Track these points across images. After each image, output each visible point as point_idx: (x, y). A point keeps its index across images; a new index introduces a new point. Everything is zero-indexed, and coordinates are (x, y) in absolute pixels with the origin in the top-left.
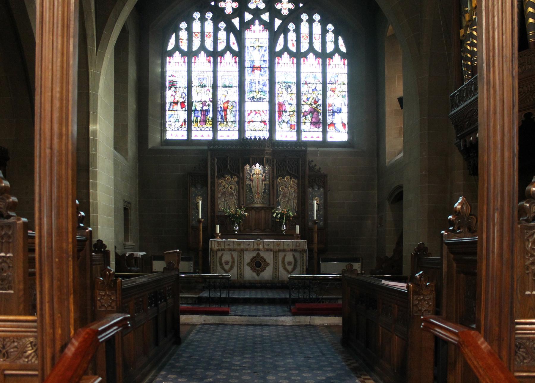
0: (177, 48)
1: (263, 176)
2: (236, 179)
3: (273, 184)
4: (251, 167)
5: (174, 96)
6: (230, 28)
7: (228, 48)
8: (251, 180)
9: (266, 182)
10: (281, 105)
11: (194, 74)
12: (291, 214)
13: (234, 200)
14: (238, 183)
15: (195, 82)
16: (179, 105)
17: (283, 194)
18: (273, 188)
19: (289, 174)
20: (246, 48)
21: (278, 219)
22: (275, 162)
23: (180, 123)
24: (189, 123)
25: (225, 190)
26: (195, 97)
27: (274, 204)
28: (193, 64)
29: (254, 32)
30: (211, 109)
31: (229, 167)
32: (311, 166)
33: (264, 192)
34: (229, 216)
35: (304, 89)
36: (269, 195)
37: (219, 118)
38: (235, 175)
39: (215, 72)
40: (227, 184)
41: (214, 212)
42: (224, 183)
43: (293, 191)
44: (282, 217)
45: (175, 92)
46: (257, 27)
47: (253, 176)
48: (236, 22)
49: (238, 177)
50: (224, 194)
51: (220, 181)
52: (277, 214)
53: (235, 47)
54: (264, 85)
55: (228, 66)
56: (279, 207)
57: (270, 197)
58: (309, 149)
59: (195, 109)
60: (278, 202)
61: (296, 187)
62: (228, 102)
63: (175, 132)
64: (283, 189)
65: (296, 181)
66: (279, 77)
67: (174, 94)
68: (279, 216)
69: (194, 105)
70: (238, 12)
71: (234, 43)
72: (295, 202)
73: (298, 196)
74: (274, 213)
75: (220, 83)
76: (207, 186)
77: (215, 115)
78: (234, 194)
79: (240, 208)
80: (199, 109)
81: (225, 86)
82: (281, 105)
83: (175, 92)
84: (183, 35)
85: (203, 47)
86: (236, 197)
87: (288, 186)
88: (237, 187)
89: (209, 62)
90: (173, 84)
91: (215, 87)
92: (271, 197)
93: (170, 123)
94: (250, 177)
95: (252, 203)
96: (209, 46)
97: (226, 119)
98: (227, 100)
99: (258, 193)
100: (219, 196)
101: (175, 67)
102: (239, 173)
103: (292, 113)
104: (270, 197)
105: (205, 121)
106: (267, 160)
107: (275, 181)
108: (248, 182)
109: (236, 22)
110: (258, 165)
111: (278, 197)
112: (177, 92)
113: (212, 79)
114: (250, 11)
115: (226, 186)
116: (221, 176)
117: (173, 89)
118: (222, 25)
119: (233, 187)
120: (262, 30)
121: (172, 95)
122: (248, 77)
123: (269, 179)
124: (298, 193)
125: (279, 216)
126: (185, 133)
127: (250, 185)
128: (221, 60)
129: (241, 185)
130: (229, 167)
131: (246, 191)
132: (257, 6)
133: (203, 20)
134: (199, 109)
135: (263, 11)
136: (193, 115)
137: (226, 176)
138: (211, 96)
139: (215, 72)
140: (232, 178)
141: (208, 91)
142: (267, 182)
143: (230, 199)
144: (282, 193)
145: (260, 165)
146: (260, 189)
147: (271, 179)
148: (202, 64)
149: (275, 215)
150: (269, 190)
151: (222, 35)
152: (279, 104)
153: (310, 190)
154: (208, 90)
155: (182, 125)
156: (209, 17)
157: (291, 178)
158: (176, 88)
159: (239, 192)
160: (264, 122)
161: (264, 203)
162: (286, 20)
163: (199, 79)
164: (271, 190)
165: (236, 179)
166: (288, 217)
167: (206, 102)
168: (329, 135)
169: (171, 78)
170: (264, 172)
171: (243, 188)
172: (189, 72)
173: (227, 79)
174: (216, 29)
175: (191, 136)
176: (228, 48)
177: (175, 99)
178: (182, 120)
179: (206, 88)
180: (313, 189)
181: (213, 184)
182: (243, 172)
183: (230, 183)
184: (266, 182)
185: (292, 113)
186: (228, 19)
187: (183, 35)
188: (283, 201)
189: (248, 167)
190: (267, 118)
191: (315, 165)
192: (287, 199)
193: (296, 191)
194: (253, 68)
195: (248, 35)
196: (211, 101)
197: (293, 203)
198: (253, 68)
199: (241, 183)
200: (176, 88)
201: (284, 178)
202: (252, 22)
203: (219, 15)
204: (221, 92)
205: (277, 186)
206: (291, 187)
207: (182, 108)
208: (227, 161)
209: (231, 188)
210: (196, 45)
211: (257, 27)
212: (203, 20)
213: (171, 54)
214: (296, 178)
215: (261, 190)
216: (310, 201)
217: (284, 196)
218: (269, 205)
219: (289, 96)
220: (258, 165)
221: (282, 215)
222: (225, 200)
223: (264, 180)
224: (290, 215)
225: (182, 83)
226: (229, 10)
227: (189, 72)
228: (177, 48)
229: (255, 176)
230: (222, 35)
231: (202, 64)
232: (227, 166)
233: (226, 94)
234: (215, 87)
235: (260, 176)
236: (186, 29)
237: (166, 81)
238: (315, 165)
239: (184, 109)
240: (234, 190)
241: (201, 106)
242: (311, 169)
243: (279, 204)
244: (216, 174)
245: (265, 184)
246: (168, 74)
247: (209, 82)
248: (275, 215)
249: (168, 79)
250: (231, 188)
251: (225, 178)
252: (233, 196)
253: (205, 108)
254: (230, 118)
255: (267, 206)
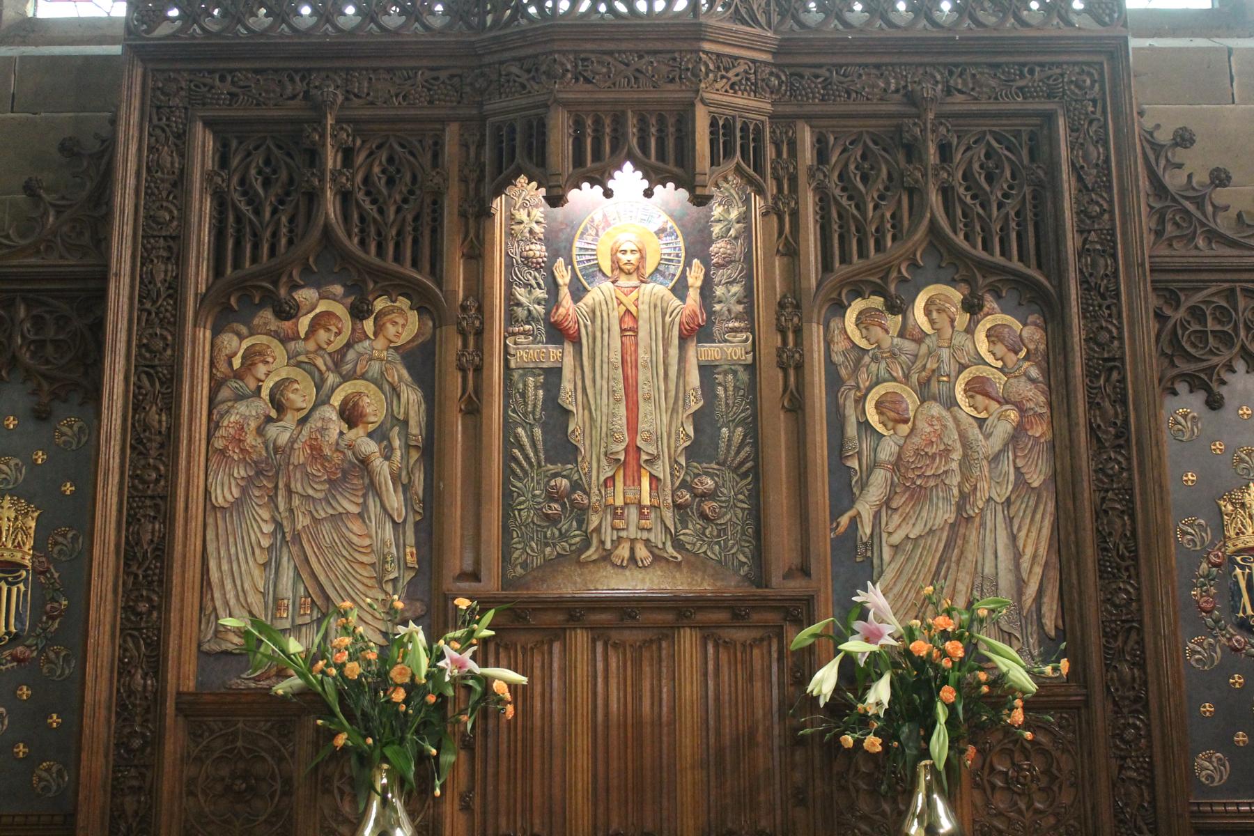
1: (680, 289)
2: (406, 325)
3: (793, 364)
4: (555, 200)
8: (558, 333)
9: (711, 352)
12: (1019, 676)
13: (379, 529)
14: (421, 361)
17: (898, 464)
18: (796, 405)
19: (949, 262)
21: (864, 721)
22: (807, 155)
25: (281, 433)
27: (805, 571)
31: (331, 207)
32: (1174, 180)
33: (692, 452)
34: (310, 700)
36: (755, 473)
38: (397, 286)
40: (310, 384)
41: (156, 665)
42: (275, 369)
43: (1002, 430)
44: (913, 706)
47: (578, 292)
49: (426, 304)
50: (269, 470)
51: (235, 345)
52: (855, 677)
56: (874, 597)
57: (757, 498)
58: (1134, 43)
60: (848, 542)
61: (1035, 397)
64: (890, 409)
65: (1032, 334)
68: (881, 692)
72: (1036, 538)
73: (1063, 485)
74: (808, 662)
76: (93, 395)
78: (382, 468)
79: (438, 620)
86: (395, 501)
87: (949, 384)
88: (412, 397)
92: (779, 498)
94: (553, 299)
95: (574, 558)
99: (631, 462)
100: (224, 493)
102: (436, 271)
104: (757, 498)
106: (723, 132)
107: (816, 333)
108: (531, 351)
110: (628, 179)
111: (844, 495)
115: (302, 395)
116: (251, 292)
119: (374, 406)
123: (749, 314)
124: (1061, 448)
125: (881, 692)
127: (554, 374)
129: (454, 384)
130: (331, 207)
131: (510, 441)
137: (306, 295)
140: (359, 312)
142: (731, 349)
143: (338, 519)
144: (887, 451)
145: (655, 176)
146: (653, 418)
147: (764, 314)
149: (825, 681)
150: (753, 428)
153: (1185, 407)
157: (972, 307)
159: (430, 451)
161: (694, 563)
164: (771, 433)
165: (406, 325)
166: (984, 704)
170: (698, 244)
171: (473, 409)
180: (1214, 403)
181: (159, 377)
182: (477, 253)
183: (338, 358)
184: (711, 352)
188: (899, 530)
189: (523, 205)
191: (1220, 178)
192: (944, 514)
193: (1039, 430)
197: (1013, 552)
199: (451, 358)
201: (898, 306)
205: (834, 381)
206: (977, 388)
208: (313, 156)
209: (351, 415)
214: (1041, 301)
215: (664, 425)
216: (1188, 532)
217: (911, 485)
218: (760, 575)
220: (628, 179)
221: (917, 682)
222: (284, 537)
223: (697, 332)
224: (999, 680)
229: (599, 292)
232: (313, 197)
235: (660, 289)
238: (1220, 178)
240: (379, 435)
242: (1180, 211)
243: (857, 563)
244: (198, 275)
245: (706, 370)
248: (825, 681)
250: (351, 415)
251: (287, 312)
252: (373, 487)
255: (731, 586)
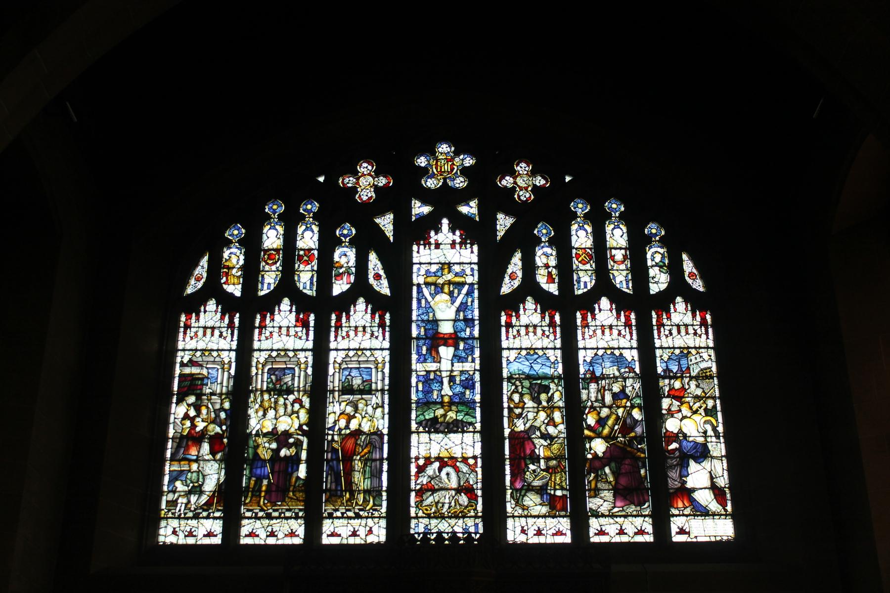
0: (213, 289)
5: (192, 420)
6: (367, 240)
7: (361, 288)
10: (521, 440)
11: (259, 357)
15: (260, 380)
16: (206, 447)
20: (415, 289)
23: (204, 499)
24: (229, 502)
26: (256, 422)
28: (257, 331)
29: (438, 246)
30: (304, 455)
35: (589, 393)
37: (327, 482)
39: (321, 351)
45: (197, 407)
46: (445, 234)
48: (386, 223)
53: (383, 288)
54: (468, 384)
55: (360, 337)
59: (256, 455)
62: (358, 432)
63: (184, 528)
66: (512, 363)
67: (192, 413)
69: (251, 443)
70: (390, 200)
71: (377, 277)
75: (334, 380)
77: (319, 473)
80: (265, 454)
81: (347, 389)
82: (521, 440)
83: (197, 407)
84: (234, 256)
85: (287, 286)
89: (305, 325)
90: (192, 385)
91: (318, 392)
93: (170, 497)
96: (305, 278)
97: (349, 483)
98: (354, 425)
101: (204, 339)
103: (553, 463)
105: (279, 492)
109: (386, 223)
112: (204, 411)
113: (310, 371)
114: (426, 196)
117: (192, 399)
118: (347, 230)
120: (458, 240)
121: (186, 416)
122: (418, 367)
126: (217, 526)
128: (339, 319)
132: (445, 183)
133: (291, 221)
134: (265, 454)
135: (464, 196)
136: (246, 472)
138: (304, 416)
139: (321, 351)
141: (297, 406)
148: (283, 334)
151: (345, 256)
152: (513, 434)
154: (298, 401)
155: (209, 504)
156: (309, 211)
158: (199, 397)
160: (468, 490)
162: (526, 216)
163: (271, 371)
167: (287, 434)
168: (676, 523)
169: (187, 370)
172: (244, 351)
173: (354, 373)
174: (328, 243)
175: (238, 536)
176: (361, 288)
177: (193, 426)
178: (210, 486)
179: (291, 398)
185: (553, 463)
186: (362, 216)
187: (234, 256)
190: (476, 479)
194: (435, 340)
195: (423, 257)
196: (304, 433)
198: (435, 340)
200: (199, 397)
202: (431, 223)
203: (338, 209)
204: (335, 409)
207: (213, 452)
210: (270, 279)
211: (445, 234)
212: (291, 221)
213: (195, 305)
219: (542, 415)
225: (221, 381)
226: (366, 194)
227: (244, 351)
228: (213, 289)
230: (345, 256)
231: (283, 334)
233: (349, 410)
234: (318, 392)
236: (242, 242)
237: (172, 377)
239: (218, 456)
241: (274, 446)
246: (182, 357)
247: (301, 379)
249: (178, 371)
253: (284, 452)
254: (361, 481)
